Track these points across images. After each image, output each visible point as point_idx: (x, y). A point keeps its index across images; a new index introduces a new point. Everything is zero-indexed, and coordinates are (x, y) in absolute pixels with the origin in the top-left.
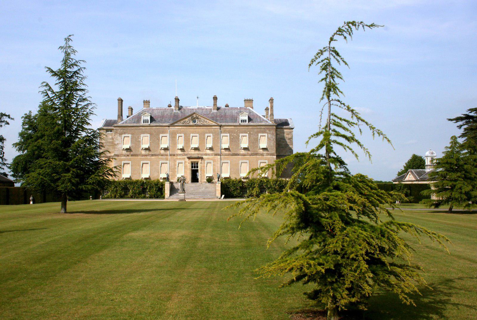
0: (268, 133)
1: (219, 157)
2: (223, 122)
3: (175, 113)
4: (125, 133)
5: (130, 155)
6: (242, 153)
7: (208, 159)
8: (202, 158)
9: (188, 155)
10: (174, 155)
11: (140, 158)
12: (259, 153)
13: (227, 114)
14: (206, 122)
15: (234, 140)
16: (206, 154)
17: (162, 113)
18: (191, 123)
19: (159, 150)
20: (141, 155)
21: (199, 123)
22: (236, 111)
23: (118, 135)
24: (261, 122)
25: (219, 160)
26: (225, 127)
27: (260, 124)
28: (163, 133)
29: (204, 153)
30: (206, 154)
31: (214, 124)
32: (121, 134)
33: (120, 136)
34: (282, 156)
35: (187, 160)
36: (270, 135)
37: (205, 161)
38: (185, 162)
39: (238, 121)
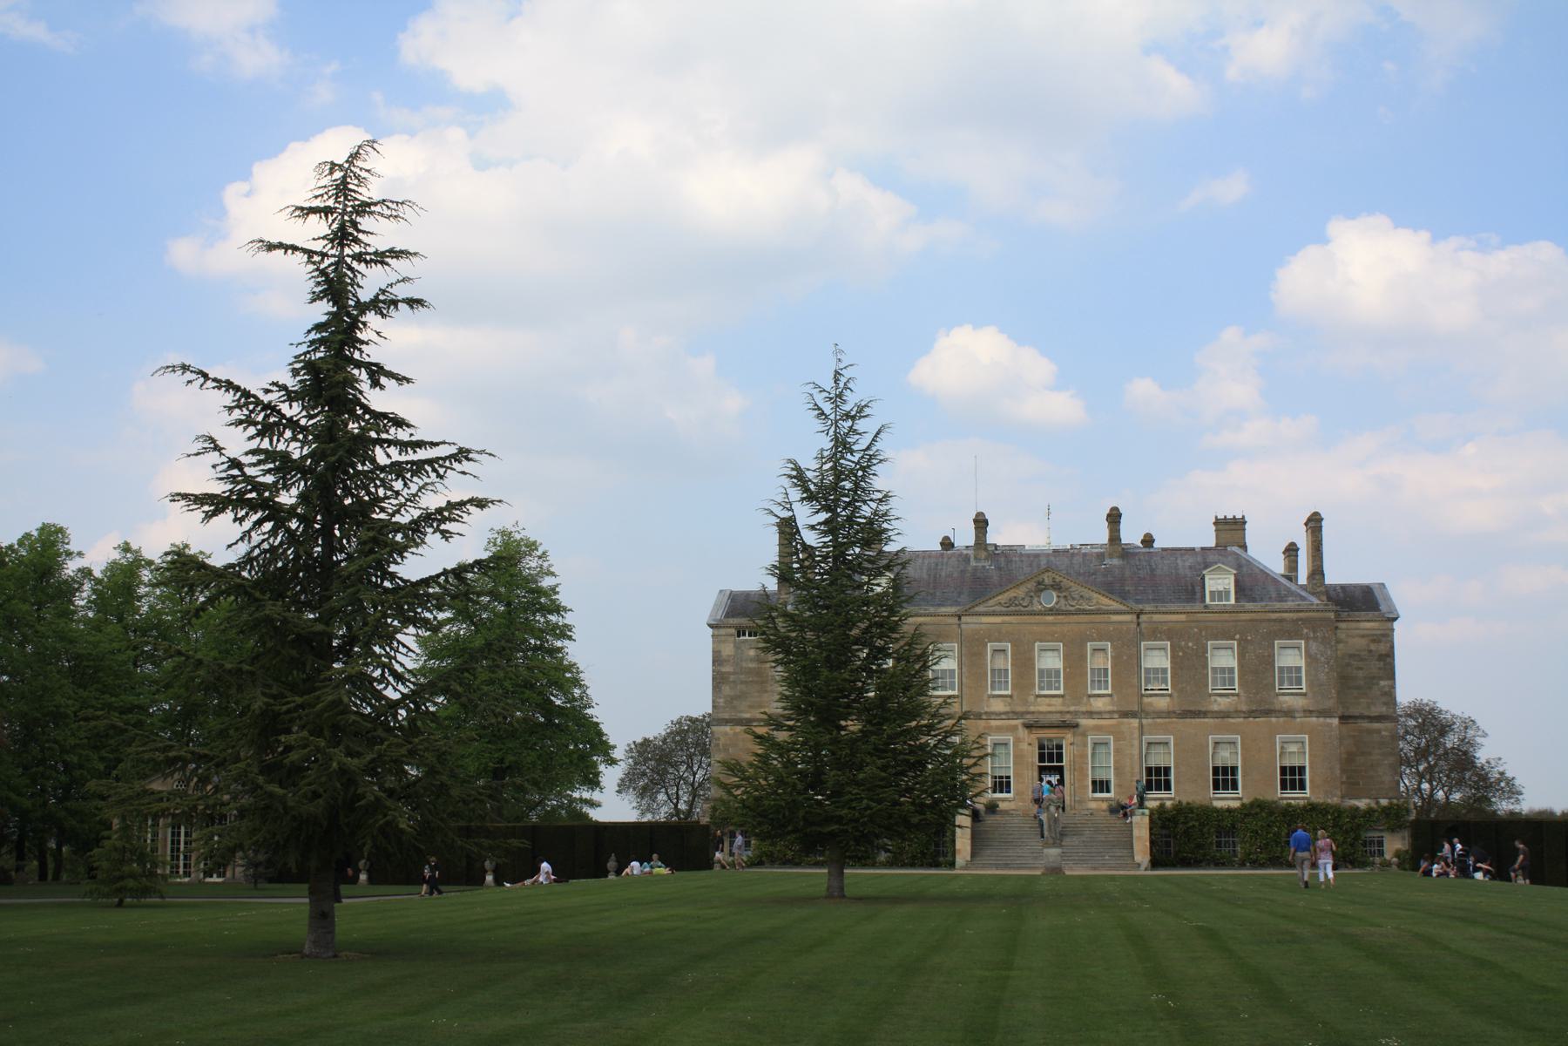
0: (1307, 639)
1: (1135, 722)
2: (1148, 601)
3: (975, 569)
6: (1216, 708)
7: (1098, 729)
8: (1077, 726)
10: (978, 716)
12: (1278, 707)
13: (1158, 572)
14: (1089, 599)
15: (1189, 664)
16: (1090, 714)
17: (929, 569)
21: (1063, 605)
22: (1190, 561)
24: (1281, 599)
25: (1136, 735)
26: (1156, 617)
27: (1278, 605)
30: (1090, 714)
31: (1115, 606)
34: (1356, 717)
36: (1314, 646)
37: (1084, 735)
38: (1017, 741)
39: (1198, 595)
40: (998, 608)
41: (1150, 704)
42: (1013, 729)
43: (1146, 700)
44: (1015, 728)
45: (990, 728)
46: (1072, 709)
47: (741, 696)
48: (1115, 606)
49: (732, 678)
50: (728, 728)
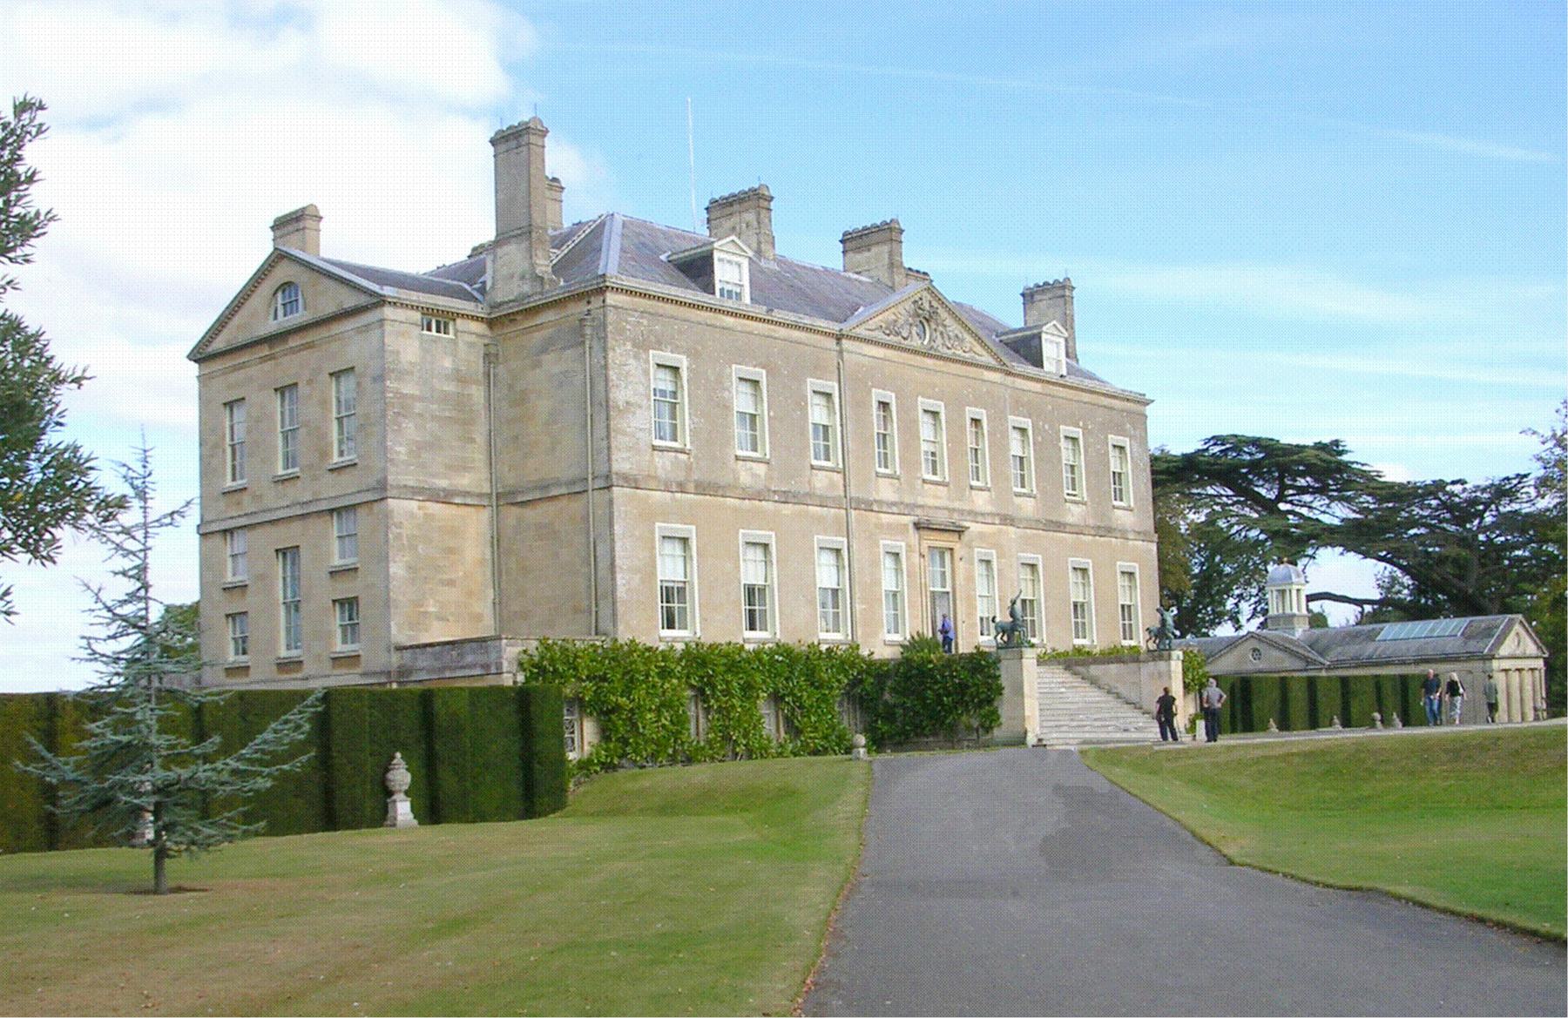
4: (659, 345)
5: (691, 486)
6: (1070, 519)
7: (982, 536)
9: (919, 511)
11: (736, 510)
16: (974, 515)
18: (915, 343)
19: (808, 472)
20: (739, 492)
23: (629, 346)
28: (818, 370)
29: (967, 507)
32: (642, 345)
33: (636, 357)
35: (913, 535)
40: (879, 335)
41: (1019, 507)
42: (900, 530)
43: (1017, 500)
44: (906, 525)
45: (879, 526)
46: (957, 505)
47: (432, 445)
48: (986, 359)
49: (418, 407)
50: (414, 505)
